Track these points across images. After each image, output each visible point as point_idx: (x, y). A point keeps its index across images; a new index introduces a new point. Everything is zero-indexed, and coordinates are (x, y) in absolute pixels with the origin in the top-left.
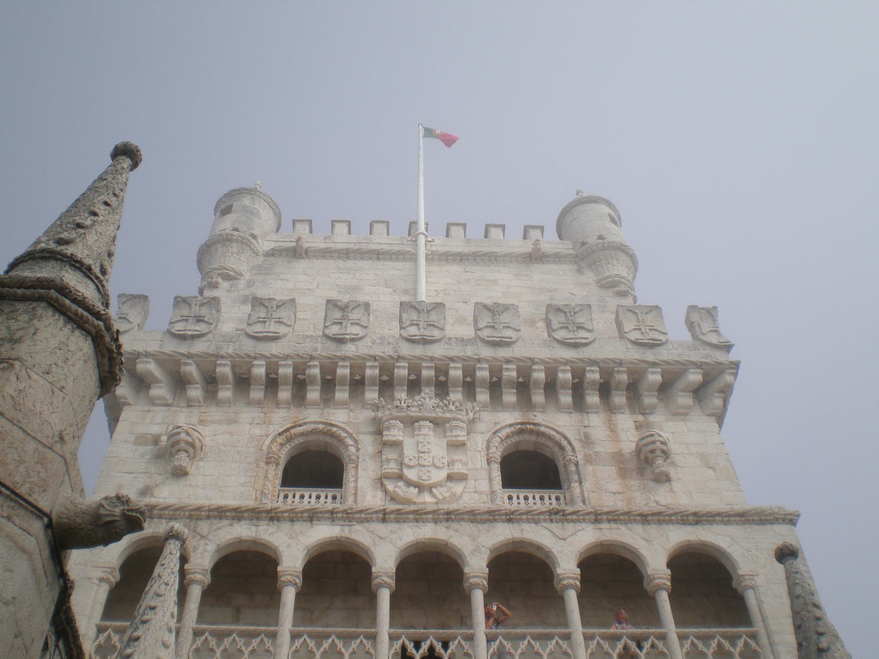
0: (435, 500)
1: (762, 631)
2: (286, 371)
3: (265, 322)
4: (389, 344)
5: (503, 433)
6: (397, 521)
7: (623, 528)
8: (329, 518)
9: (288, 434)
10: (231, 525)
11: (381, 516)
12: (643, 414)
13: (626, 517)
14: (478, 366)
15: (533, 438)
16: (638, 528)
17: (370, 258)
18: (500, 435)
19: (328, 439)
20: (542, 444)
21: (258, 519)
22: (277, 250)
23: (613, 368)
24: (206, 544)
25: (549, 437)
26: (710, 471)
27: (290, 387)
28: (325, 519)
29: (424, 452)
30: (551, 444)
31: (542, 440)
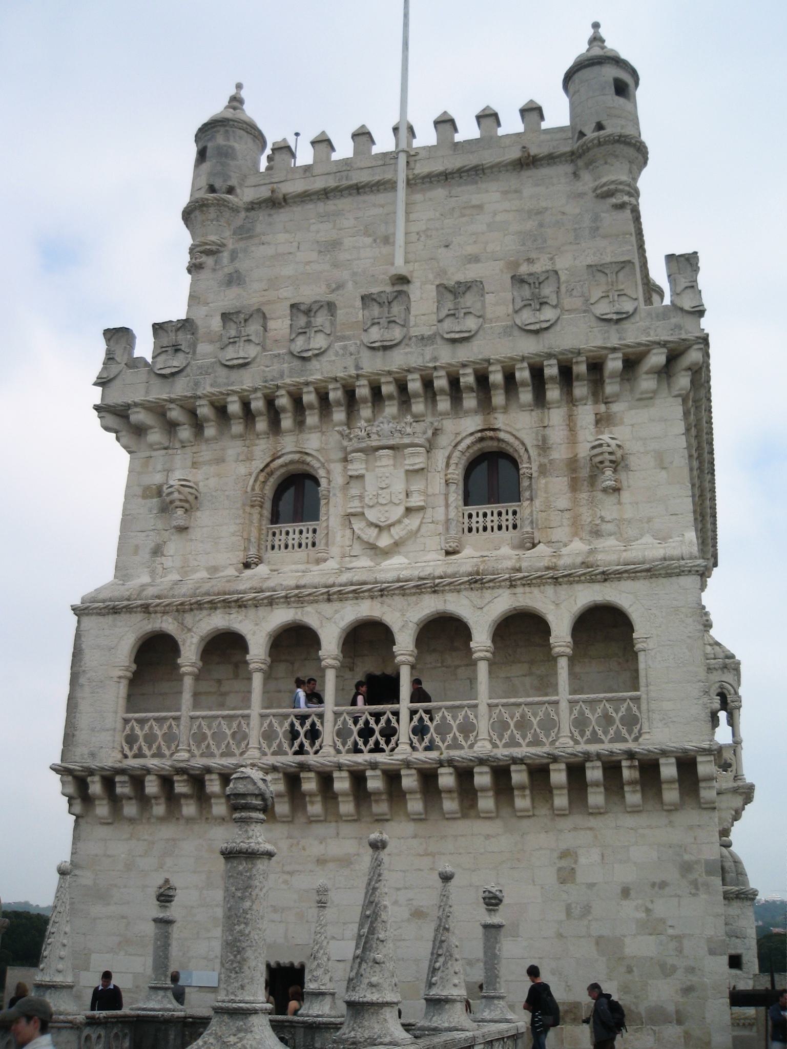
0: (392, 541)
1: (644, 696)
2: (258, 404)
4: (351, 354)
7: (536, 591)
9: (268, 470)
10: (210, 615)
11: (325, 597)
12: (606, 403)
13: (539, 581)
14: (435, 374)
16: (550, 590)
17: (350, 194)
18: (460, 448)
19: (305, 467)
21: (230, 607)
22: (256, 204)
23: (572, 359)
26: (664, 474)
27: (265, 418)
29: (382, 489)
31: (504, 446)
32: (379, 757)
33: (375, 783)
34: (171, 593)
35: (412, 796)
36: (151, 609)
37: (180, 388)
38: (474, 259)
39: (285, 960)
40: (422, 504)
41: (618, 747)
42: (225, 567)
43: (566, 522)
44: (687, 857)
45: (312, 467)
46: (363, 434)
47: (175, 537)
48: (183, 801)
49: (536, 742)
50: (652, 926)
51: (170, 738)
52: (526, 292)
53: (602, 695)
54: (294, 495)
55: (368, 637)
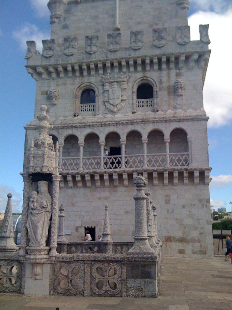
1: (190, 154)
2: (77, 67)
3: (69, 48)
5: (137, 82)
6: (105, 126)
7: (160, 124)
9: (80, 87)
11: (101, 125)
14: (130, 60)
15: (146, 81)
16: (164, 124)
18: (136, 82)
19: (90, 87)
21: (72, 128)
24: (62, 136)
25: (150, 81)
26: (195, 91)
28: (88, 127)
29: (114, 94)
31: (149, 82)
32: (116, 170)
33: (115, 177)
34: (54, 124)
37: (52, 61)
38: (140, 23)
39: (90, 226)
40: (126, 99)
41: (183, 167)
42: (69, 116)
44: (200, 198)
45: (93, 87)
46: (109, 78)
50: (191, 216)
52: (157, 34)
54: (88, 96)
55: (113, 136)
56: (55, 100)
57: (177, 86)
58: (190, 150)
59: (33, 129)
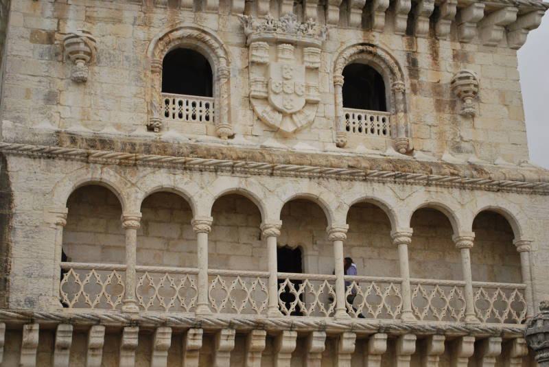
0: (295, 128)
1: (529, 288)
6: (282, 176)
7: (445, 191)
8: (230, 171)
9: (166, 39)
10: (154, 173)
11: (270, 171)
12: (461, 42)
13: (449, 183)
16: (456, 192)
19: (199, 44)
20: (376, 63)
21: (174, 168)
24: (137, 192)
25: (384, 60)
26: (505, 109)
28: (227, 171)
29: (287, 79)
30: (383, 66)
31: (376, 60)
33: (318, 344)
35: (344, 358)
36: (91, 158)
40: (316, 99)
43: (434, 136)
45: (210, 46)
47: (73, 88)
48: (123, 353)
49: (449, 317)
51: (116, 289)
53: (498, 284)
55: (303, 211)
56: (88, 63)
57: (466, 88)
58: (527, 275)
59: (32, 155)
